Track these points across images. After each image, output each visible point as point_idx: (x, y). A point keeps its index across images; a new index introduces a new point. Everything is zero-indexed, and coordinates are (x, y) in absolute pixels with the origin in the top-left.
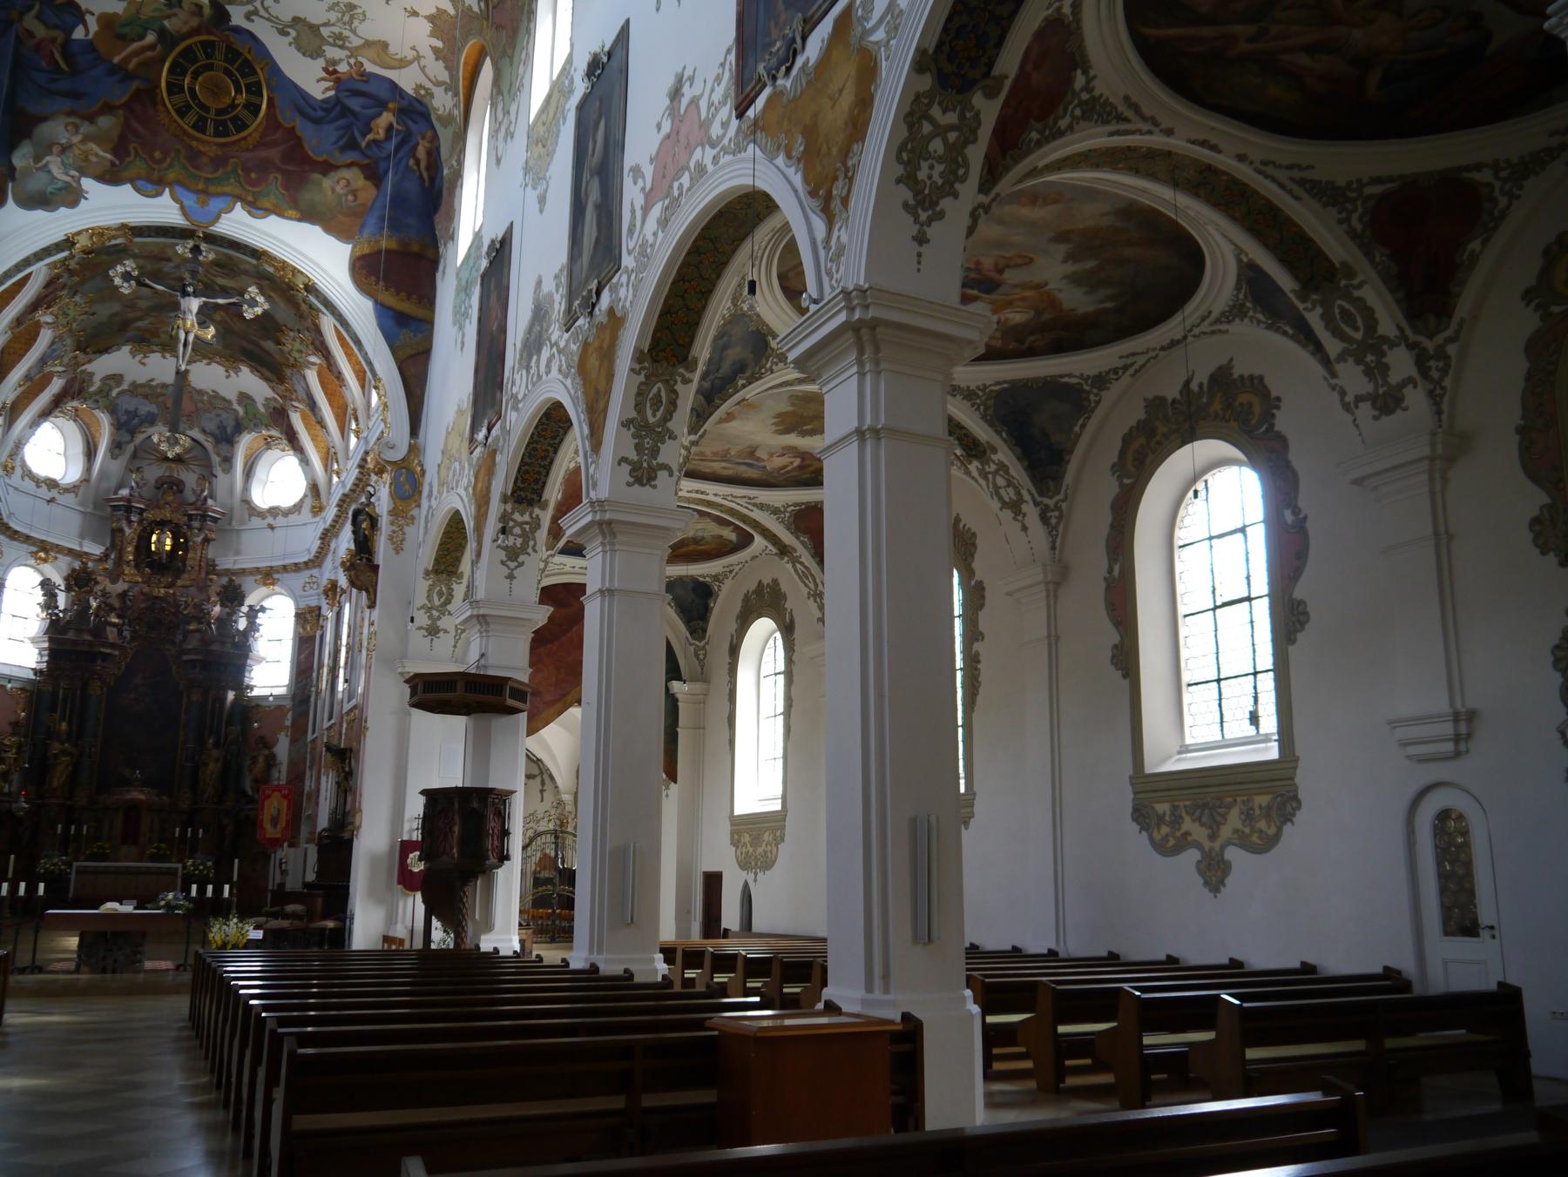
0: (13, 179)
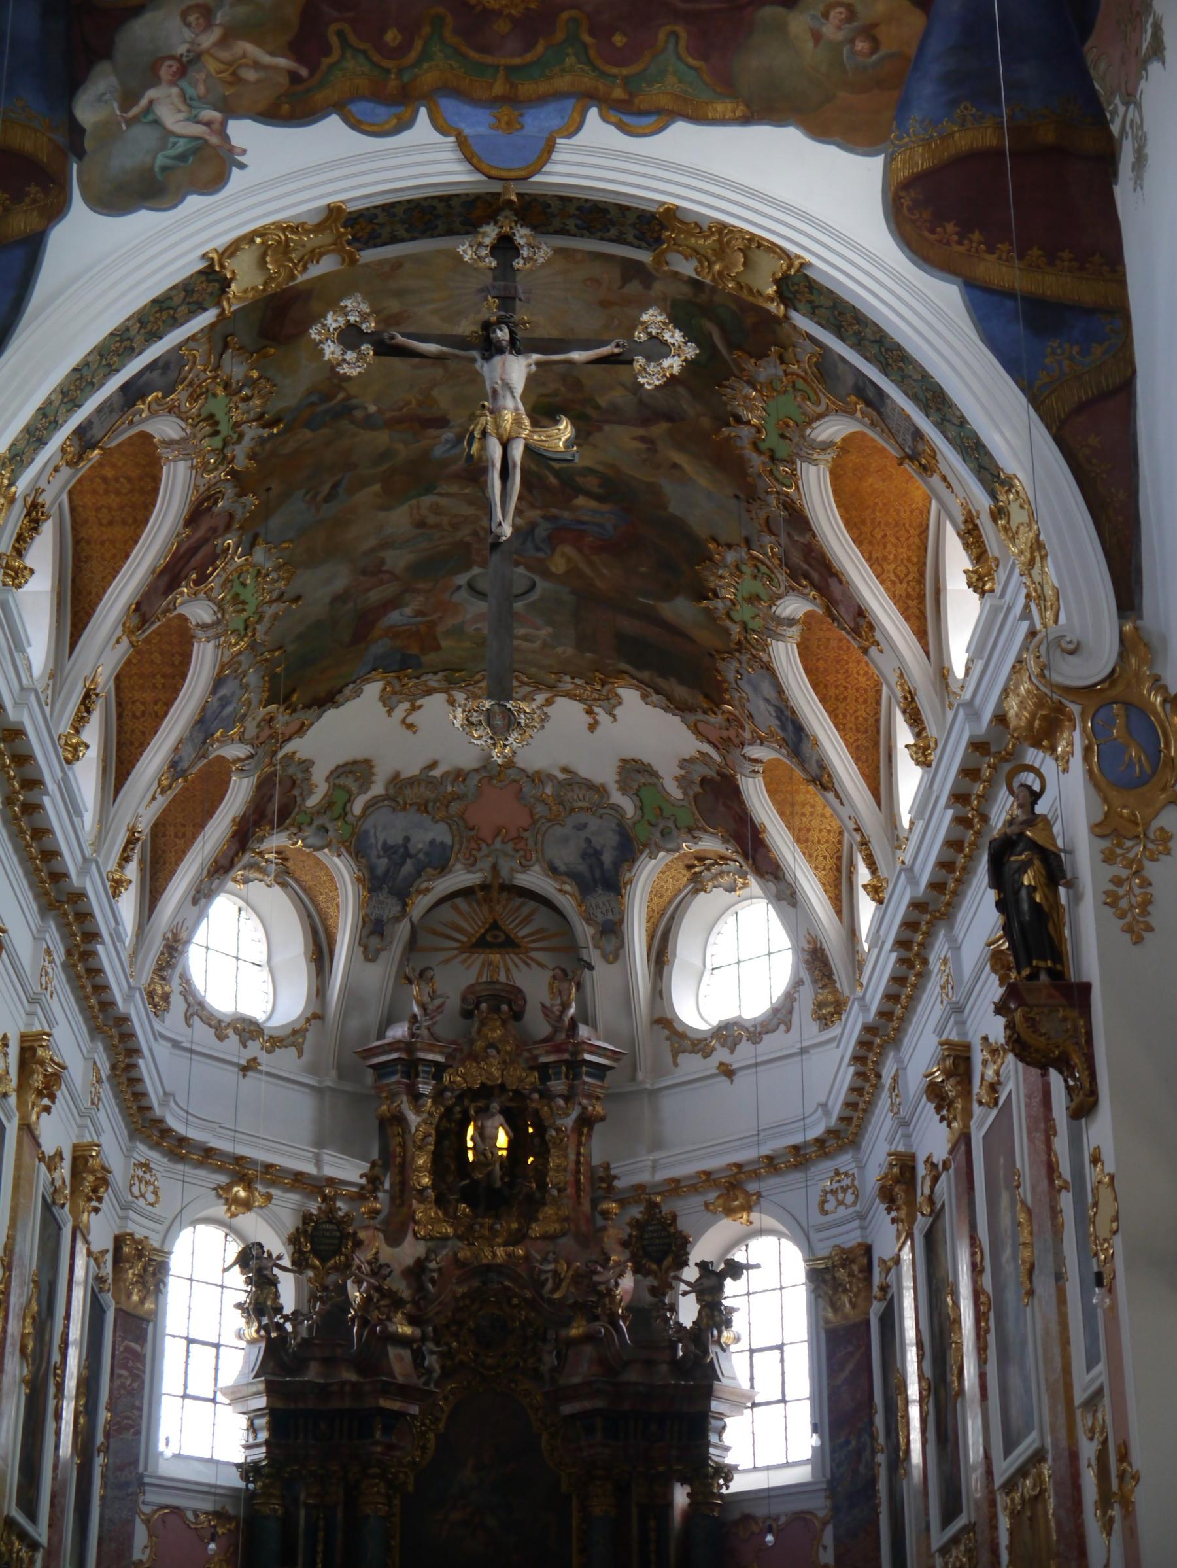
0: (80, 154)
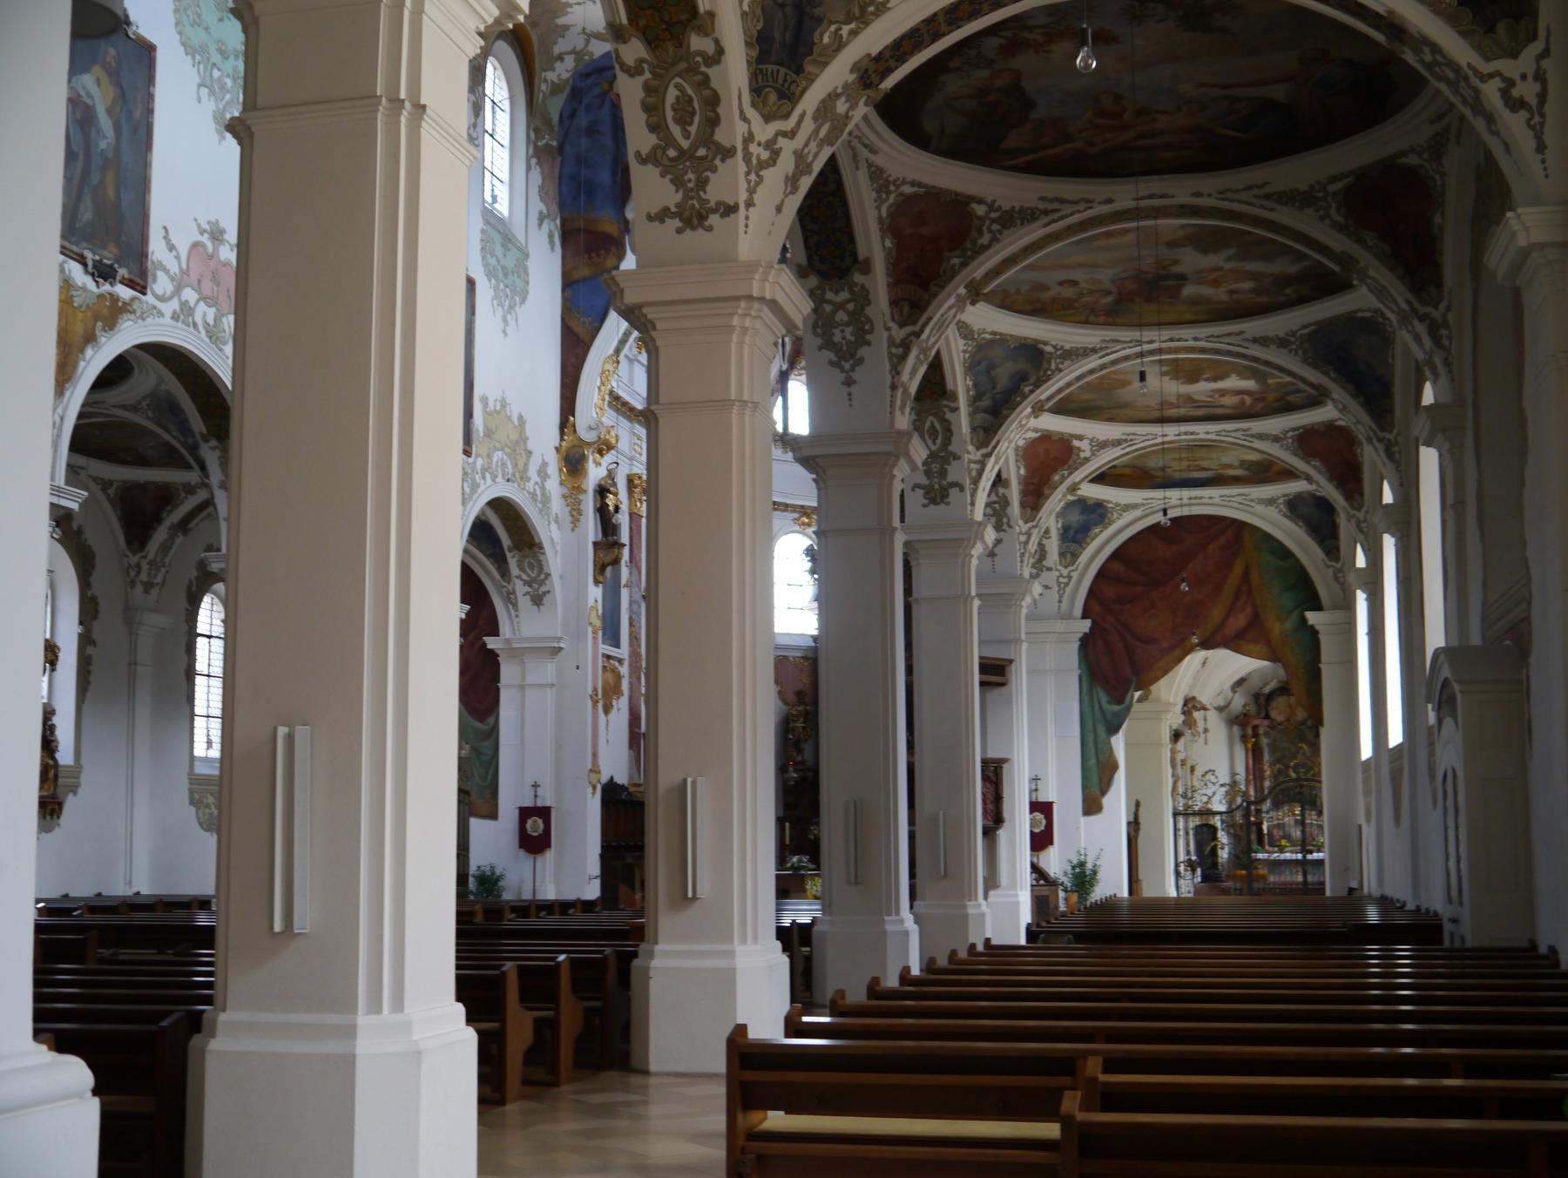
0: (628, 231)
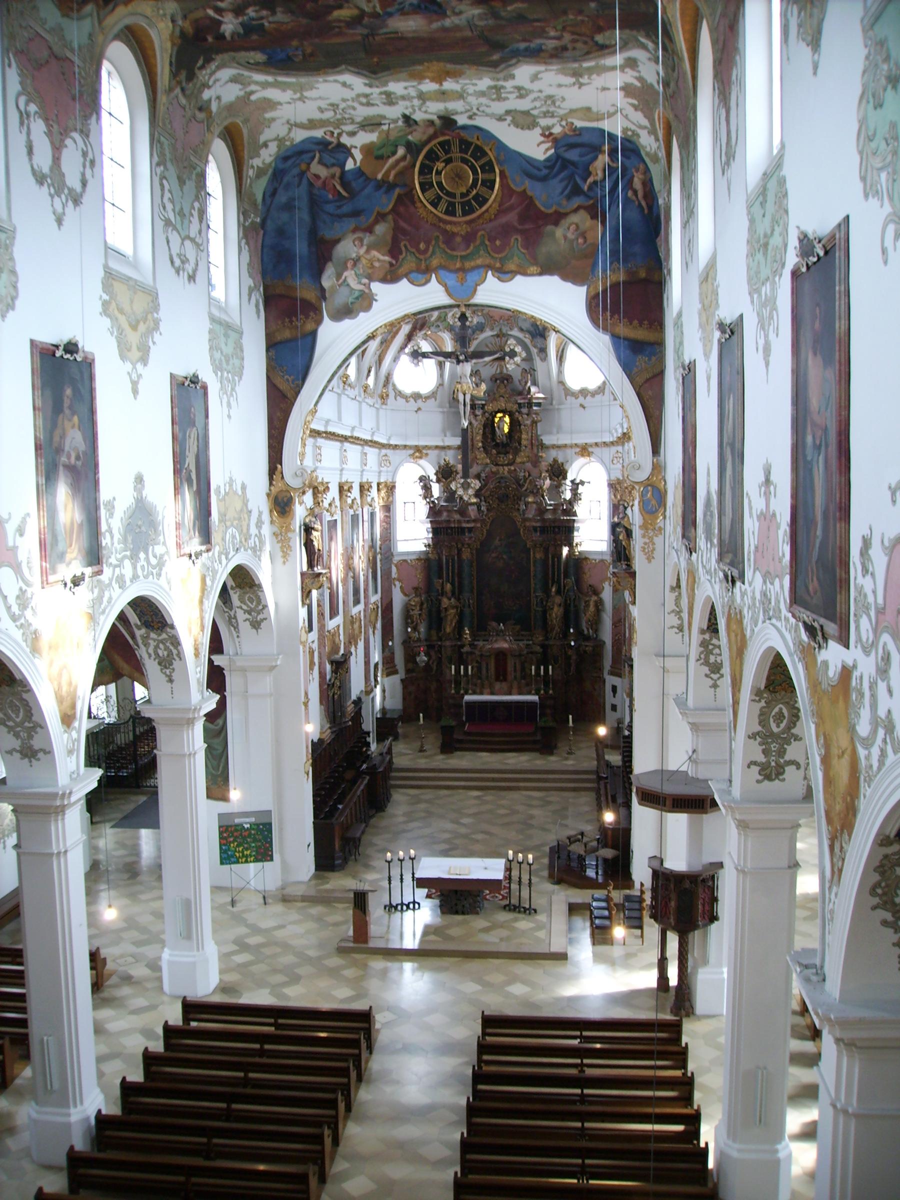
0: (325, 298)
